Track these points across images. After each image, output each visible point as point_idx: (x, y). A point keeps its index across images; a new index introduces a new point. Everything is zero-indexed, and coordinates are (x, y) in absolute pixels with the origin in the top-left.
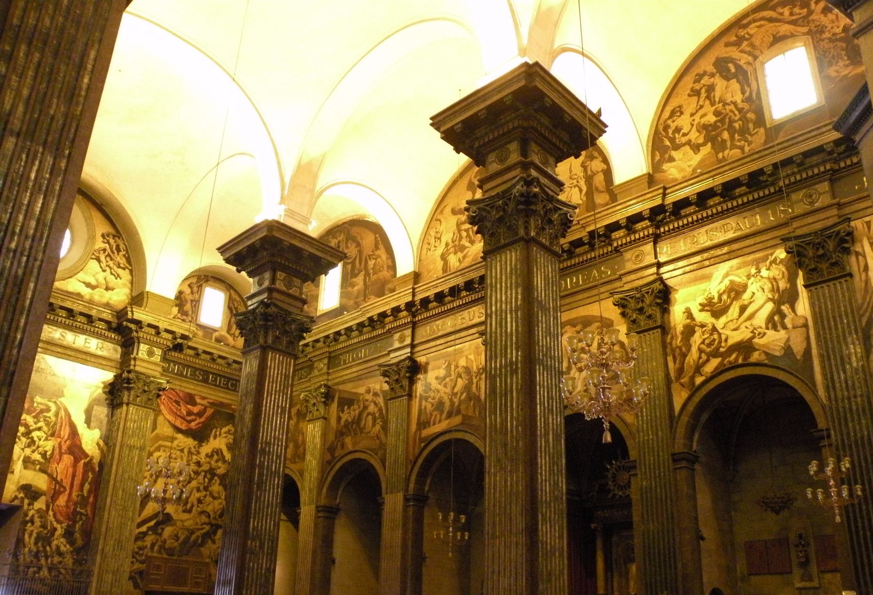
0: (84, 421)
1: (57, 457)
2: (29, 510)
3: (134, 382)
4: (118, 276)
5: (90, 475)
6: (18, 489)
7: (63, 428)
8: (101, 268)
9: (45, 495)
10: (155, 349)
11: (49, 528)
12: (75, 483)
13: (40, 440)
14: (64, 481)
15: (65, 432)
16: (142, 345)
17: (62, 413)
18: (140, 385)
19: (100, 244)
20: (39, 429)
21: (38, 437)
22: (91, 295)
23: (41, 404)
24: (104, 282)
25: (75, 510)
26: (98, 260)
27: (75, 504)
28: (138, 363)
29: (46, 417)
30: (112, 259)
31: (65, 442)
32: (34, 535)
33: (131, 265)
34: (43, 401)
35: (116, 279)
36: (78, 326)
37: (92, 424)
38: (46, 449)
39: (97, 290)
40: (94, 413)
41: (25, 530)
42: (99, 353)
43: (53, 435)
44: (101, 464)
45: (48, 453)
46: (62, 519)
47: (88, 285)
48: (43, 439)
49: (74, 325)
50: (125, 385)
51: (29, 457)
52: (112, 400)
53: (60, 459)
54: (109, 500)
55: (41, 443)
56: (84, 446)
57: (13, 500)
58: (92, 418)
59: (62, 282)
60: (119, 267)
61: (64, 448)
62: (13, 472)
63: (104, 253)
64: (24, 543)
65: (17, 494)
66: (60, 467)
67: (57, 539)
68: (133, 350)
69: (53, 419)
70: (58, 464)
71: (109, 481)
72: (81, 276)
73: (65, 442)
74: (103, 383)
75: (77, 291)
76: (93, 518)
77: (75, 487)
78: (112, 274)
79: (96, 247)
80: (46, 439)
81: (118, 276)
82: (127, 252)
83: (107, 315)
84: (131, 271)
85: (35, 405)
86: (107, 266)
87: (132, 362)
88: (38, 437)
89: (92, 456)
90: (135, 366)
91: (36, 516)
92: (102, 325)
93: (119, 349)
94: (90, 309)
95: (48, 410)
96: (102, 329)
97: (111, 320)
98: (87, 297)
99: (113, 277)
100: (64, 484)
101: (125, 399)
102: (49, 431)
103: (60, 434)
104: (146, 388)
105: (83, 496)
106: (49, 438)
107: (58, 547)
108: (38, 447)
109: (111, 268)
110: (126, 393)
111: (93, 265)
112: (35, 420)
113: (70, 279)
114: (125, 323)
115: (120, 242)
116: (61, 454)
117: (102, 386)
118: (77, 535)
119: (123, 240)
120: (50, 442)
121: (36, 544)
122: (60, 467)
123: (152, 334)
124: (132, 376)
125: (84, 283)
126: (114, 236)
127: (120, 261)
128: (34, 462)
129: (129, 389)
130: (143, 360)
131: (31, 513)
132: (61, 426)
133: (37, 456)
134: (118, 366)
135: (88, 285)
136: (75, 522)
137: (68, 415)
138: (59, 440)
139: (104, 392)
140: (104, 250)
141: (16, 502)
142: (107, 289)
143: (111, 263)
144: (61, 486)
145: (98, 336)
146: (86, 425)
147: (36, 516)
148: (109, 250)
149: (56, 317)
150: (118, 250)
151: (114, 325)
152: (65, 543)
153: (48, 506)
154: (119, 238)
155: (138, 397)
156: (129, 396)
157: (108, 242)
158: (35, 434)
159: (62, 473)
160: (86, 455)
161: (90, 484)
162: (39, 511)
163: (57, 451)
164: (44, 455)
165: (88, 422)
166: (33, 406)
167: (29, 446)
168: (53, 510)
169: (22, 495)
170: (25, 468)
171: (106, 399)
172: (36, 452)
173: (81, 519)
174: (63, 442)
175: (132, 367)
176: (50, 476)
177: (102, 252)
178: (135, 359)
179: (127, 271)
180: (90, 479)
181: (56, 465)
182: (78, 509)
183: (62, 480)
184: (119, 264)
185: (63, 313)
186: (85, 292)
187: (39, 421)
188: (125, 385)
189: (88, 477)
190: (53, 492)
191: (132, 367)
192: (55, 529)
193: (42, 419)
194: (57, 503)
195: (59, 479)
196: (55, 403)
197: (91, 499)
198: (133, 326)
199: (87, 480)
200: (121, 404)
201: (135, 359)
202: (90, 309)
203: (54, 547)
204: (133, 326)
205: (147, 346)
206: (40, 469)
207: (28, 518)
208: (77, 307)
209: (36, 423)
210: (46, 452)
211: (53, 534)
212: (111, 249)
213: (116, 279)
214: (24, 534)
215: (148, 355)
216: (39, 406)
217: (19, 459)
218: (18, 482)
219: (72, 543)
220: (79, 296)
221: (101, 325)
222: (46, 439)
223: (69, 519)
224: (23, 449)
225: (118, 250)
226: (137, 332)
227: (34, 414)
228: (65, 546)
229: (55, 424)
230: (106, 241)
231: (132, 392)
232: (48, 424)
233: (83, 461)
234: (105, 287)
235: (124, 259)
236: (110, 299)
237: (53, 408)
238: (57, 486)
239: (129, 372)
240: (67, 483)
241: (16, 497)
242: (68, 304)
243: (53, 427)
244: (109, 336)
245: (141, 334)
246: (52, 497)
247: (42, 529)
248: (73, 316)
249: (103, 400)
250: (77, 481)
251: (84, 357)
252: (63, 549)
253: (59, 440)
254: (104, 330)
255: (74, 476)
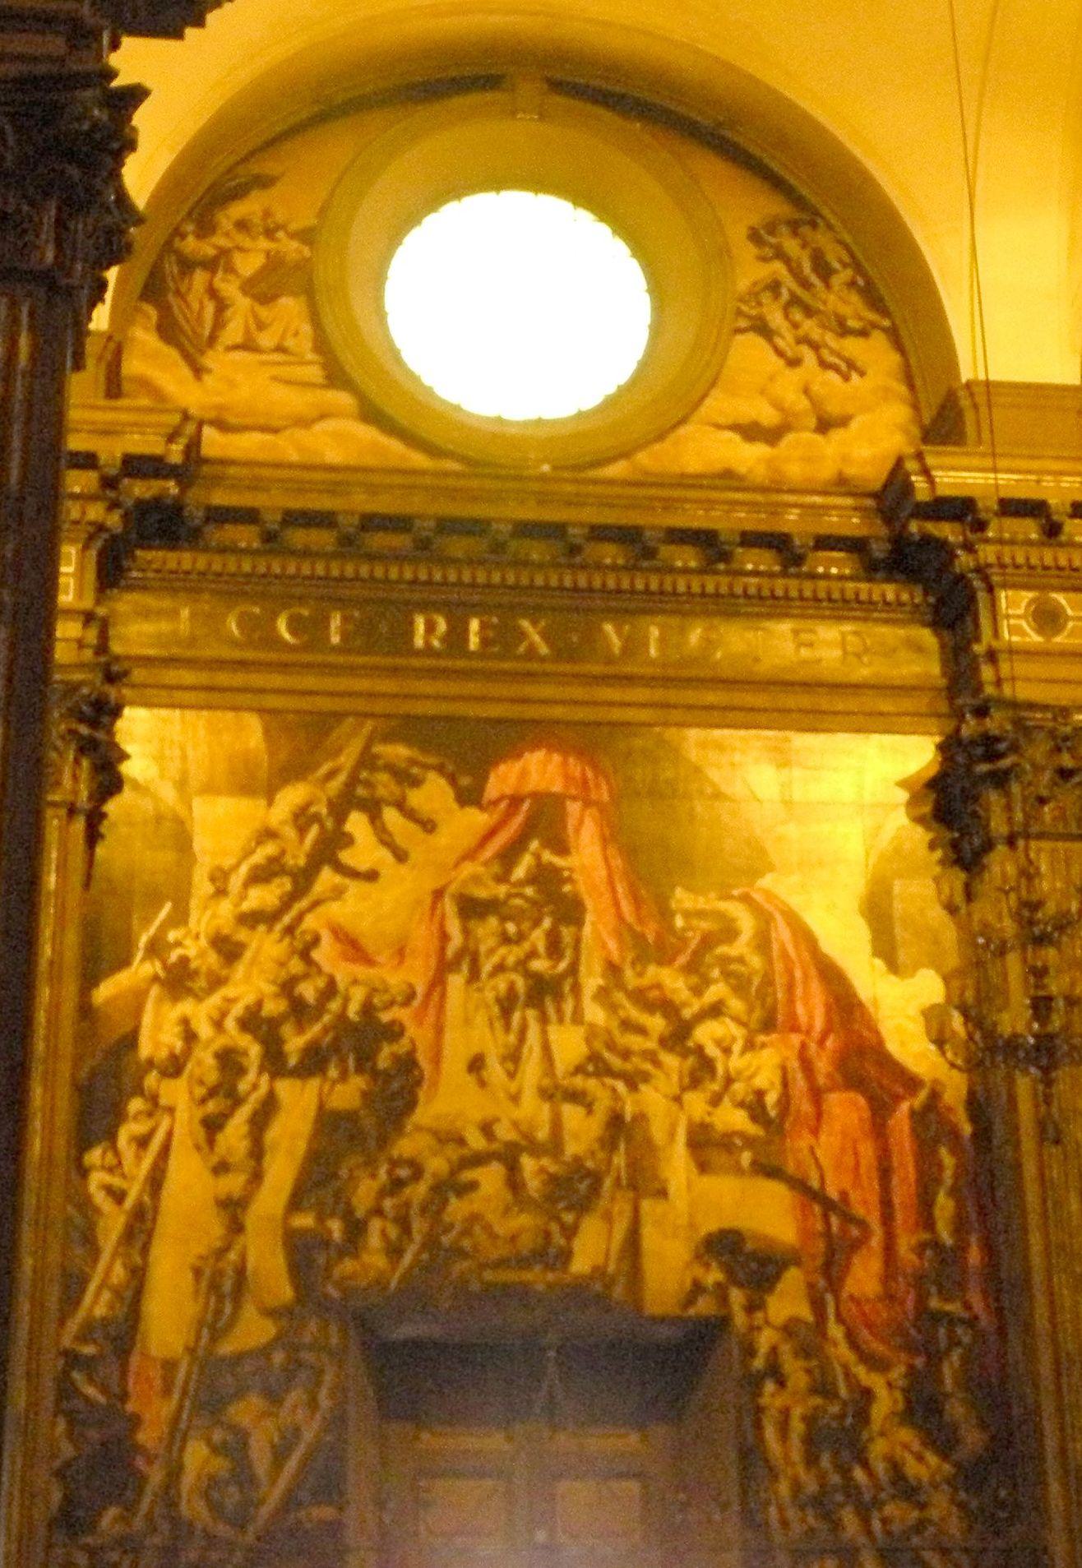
0: (867, 948)
1: (806, 1107)
2: (754, 1329)
3: (1015, 748)
4: (850, 368)
5: (948, 1159)
6: (698, 1257)
7: (799, 991)
8: (780, 353)
9: (798, 1263)
10: (1060, 598)
11: (843, 1391)
12: (896, 1200)
13: (727, 1051)
14: (854, 1196)
15: (812, 1008)
16: (1003, 596)
17: (782, 933)
18: (1038, 751)
19: (751, 270)
20: (716, 1011)
21: (718, 1043)
22: (769, 462)
23: (701, 914)
24: (804, 404)
25: (921, 1300)
26: (763, 329)
27: (919, 1281)
28: (1005, 668)
29: (725, 961)
30: (809, 312)
31: (821, 1042)
32: (797, 1427)
33: (885, 312)
34: (701, 903)
35: (846, 378)
36: (752, 591)
37: (902, 956)
38: (760, 1082)
39: (790, 438)
40: (898, 907)
41: (759, 1410)
42: (863, 672)
43: (768, 1025)
44: (976, 1106)
45: (771, 1099)
46: (878, 1347)
47: (751, 432)
48: (737, 1048)
49: (739, 590)
50: (983, 768)
51: (705, 1127)
52: (955, 845)
53: (819, 1115)
54: (1036, 1241)
55: (736, 1062)
56: (893, 1047)
57: (690, 1300)
58: (898, 931)
59: (657, 447)
60: (844, 331)
61: (823, 1066)
62: (663, 1193)
63: (776, 295)
64: (767, 1461)
65: (698, 1271)
66: (828, 1145)
67: (882, 1434)
68: (977, 625)
69: (756, 962)
70: (815, 1132)
71: (1018, 1166)
72: (718, 405)
73: (821, 1042)
74: (903, 784)
75: (718, 467)
76: (1002, 1331)
77: (899, 1216)
78: (824, 365)
79: (743, 284)
80: (750, 1046)
81: (851, 365)
82: (858, 267)
83: (847, 520)
84: (898, 345)
85: (679, 922)
86: (800, 341)
87: (987, 673)
88: (718, 1043)
89: (936, 1082)
90: (998, 682)
91: (786, 1349)
92: (835, 565)
93: (927, 637)
94: (776, 510)
95: (730, 932)
96: (841, 578)
97: (863, 532)
98: (760, 474)
99: (832, 376)
100: (859, 1211)
101: (998, 825)
102: (751, 1010)
103: (792, 1015)
104: (1067, 761)
105: (936, 1245)
106: (761, 1038)
107: (896, 1467)
108: (729, 1081)
109: (815, 347)
110: (994, 798)
111: (750, 353)
112: (694, 980)
113: (682, 431)
114: (914, 527)
115: (822, 239)
116: (817, 1095)
117: (903, 796)
118: (956, 1409)
119: (830, 227)
120: (766, 1053)
121: (811, 1460)
122: (828, 1145)
123: (1029, 543)
124: (996, 722)
125: (736, 428)
126: (794, 227)
127: (845, 310)
128: (727, 1143)
129: (1000, 780)
130: (1029, 653)
131: (765, 1339)
132: (790, 987)
133: (731, 1118)
134: (944, 707)
135: (751, 432)
136: (935, 1358)
137: (806, 938)
138: (796, 1039)
139: (919, 820)
140: (774, 287)
141: (705, 1306)
142: (825, 425)
143: (810, 327)
144: (848, 1218)
145: (840, 608)
146: (879, 963)
147: (786, 1349)
148: (789, 283)
149: (668, 580)
150: (824, 270)
151: (879, 550)
152: (916, 1446)
153: (818, 1306)
154: (814, 225)
155: (1042, 801)
156: (1009, 808)
157: (780, 254)
158: (706, 1034)
159: (838, 1165)
160: (912, 1083)
161: (954, 1192)
162: (789, 1329)
163: (800, 1082)
164: (755, 1107)
165: (886, 949)
166: (671, 928)
167: (695, 1082)
168: (840, 1319)
169: (714, 1276)
170: (703, 1167)
171: (932, 846)
172: (726, 1101)
173: (954, 1342)
174: (813, 1047)
175: (989, 690)
176: (799, 1185)
177: (766, 297)
178: (992, 656)
179: (879, 340)
180: (948, 1175)
181: (812, 1141)
182: (934, 1303)
183: (844, 1195)
184: (841, 322)
185: (687, 557)
186: (749, 457)
187: (707, 982)
188: (983, 768)
189: (940, 1166)
190: (821, 1245)
191: (989, 690)
192: (867, 1394)
193: (716, 973)
194: (851, 1286)
195: (833, 1193)
196: (746, 899)
197: (974, 1256)
198: (948, 531)
199: (938, 1181)
200: (988, 846)
201: (992, 656)
202: (776, 510)
203: (880, 1467)
204: (948, 531)
205: (1027, 596)
206: (754, 1163)
207: (758, 1363)
208: (728, 520)
209: (697, 991)
210: (760, 1094)
211: (863, 1416)
212: (796, 272)
213: (846, 378)
214: (758, 1426)
215: (1040, 630)
216: (695, 922)
217: (672, 1135)
218: (692, 1226)
219: (942, 1440)
220: (728, 478)
221: (834, 562)
222: (750, 1046)
223: (910, 1348)
224: (677, 1099)
225: (824, 270)
226: (969, 547)
227: (682, 959)
228: (920, 1458)
229: (768, 981)
230: (769, 252)
231: (1015, 788)
232: (740, 985)
233: (905, 1106)
234: (812, 422)
235: (855, 298)
236: (845, 459)
237: (746, 924)
238: (835, 1221)
239: (982, 712)
240: (865, 1206)
241: (698, 1288)
242: (694, 518)
243: (762, 995)
244: (876, 597)
245: (988, 553)
246: (828, 1266)
247: (817, 1401)
248: (725, 557)
249: (922, 850)
250: (903, 1189)
251: (805, 701)
252: (912, 1469)
253: (796, 1039)
254: (851, 578)
255: (885, 1173)
